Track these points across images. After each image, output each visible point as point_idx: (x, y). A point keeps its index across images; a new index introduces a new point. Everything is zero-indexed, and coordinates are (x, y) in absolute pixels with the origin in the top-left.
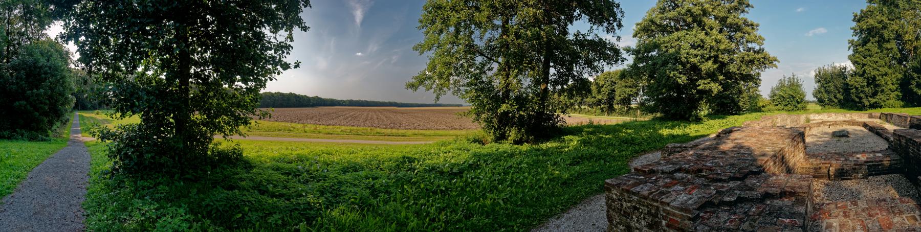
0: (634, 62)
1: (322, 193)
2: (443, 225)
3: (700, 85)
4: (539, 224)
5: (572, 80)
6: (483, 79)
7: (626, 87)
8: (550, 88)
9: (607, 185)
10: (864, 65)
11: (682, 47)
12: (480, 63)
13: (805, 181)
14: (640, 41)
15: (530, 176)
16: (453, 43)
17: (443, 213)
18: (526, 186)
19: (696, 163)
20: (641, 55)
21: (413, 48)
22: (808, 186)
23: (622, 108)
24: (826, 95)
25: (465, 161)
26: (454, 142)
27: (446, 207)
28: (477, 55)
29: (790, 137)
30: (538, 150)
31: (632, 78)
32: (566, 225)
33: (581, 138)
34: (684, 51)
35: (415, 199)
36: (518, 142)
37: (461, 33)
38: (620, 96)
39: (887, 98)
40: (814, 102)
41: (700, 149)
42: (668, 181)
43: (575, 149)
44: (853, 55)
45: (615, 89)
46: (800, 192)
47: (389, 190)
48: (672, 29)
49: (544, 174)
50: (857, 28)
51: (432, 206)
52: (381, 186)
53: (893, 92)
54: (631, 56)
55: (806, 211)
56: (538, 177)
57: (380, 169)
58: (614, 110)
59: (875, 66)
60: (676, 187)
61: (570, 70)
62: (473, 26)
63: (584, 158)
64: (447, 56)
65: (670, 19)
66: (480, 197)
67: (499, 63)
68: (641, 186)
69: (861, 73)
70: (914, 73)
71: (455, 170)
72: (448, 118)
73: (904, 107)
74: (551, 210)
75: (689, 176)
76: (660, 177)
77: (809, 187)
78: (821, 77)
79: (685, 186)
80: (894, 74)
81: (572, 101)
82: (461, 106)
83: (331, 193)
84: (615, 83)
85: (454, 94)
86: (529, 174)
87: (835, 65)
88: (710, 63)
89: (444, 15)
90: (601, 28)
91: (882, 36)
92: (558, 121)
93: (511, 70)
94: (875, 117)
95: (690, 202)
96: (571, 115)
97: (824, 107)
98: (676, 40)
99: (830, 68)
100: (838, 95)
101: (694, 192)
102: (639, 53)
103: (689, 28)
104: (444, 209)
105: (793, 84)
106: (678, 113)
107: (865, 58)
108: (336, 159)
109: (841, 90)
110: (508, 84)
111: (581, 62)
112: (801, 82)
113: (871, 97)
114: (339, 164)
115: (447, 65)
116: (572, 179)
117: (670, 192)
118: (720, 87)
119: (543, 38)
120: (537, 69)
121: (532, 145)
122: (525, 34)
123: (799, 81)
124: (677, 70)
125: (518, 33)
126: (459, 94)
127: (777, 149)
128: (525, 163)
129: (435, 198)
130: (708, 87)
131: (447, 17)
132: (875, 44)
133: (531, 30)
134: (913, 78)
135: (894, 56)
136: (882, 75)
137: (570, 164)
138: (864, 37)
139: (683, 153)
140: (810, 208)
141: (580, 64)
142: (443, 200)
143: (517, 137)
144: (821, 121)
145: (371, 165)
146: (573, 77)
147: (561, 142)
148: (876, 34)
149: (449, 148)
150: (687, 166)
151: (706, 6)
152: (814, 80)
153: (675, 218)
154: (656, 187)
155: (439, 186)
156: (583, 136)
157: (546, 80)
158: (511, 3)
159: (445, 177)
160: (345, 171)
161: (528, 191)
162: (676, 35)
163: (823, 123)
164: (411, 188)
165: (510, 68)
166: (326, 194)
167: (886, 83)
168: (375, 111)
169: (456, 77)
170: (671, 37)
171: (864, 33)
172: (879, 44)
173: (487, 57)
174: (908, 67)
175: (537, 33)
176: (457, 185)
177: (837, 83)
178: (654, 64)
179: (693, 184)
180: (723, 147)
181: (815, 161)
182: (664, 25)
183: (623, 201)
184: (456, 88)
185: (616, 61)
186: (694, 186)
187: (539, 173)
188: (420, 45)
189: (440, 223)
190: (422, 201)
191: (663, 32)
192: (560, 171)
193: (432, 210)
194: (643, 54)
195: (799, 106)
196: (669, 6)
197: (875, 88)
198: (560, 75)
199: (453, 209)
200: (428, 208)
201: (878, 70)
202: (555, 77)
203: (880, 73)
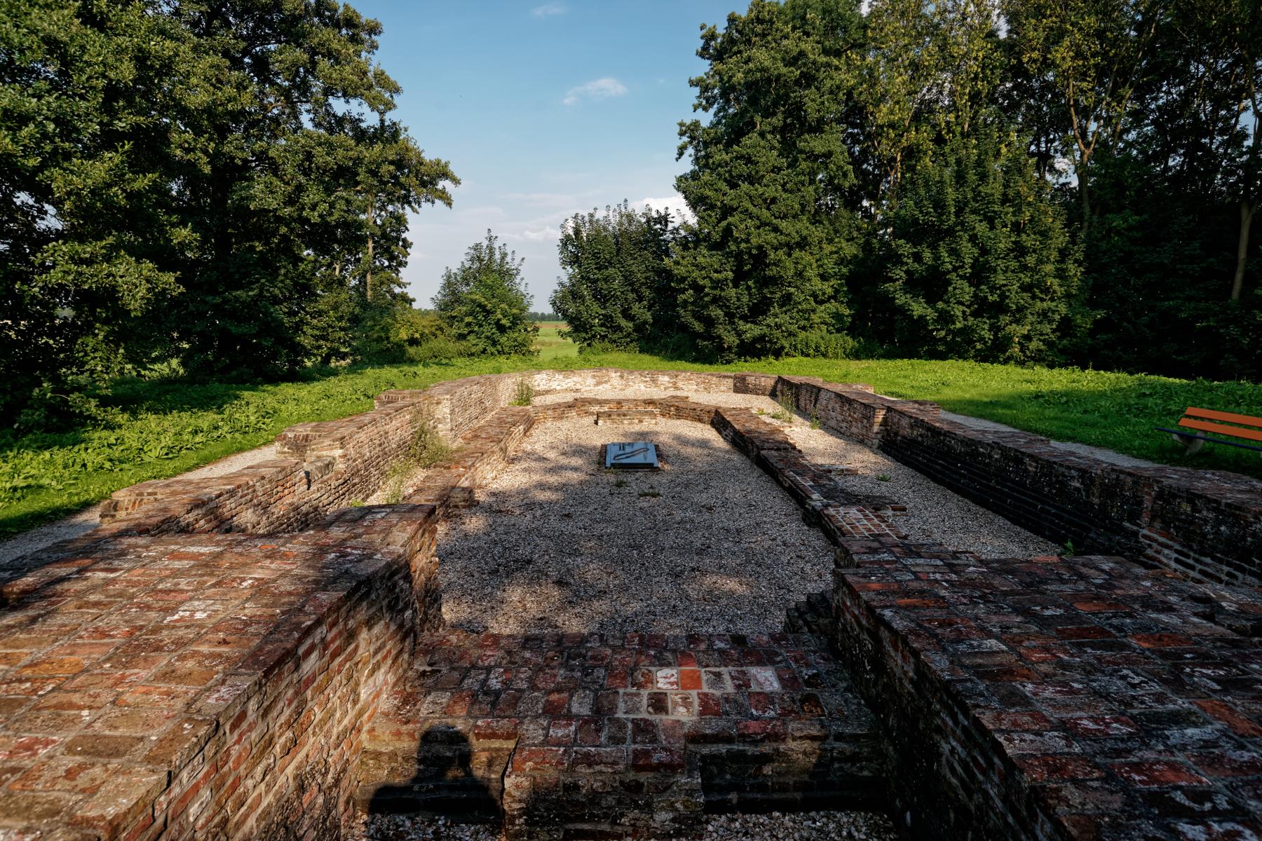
10: (727, 211)
24: (596, 307)
39: (802, 323)
44: (694, 176)
50: (711, 81)
53: (822, 302)
59: (765, 214)
69: (716, 237)
70: (902, 241)
73: (856, 355)
80: (830, 241)
87: (630, 209)
91: (796, 110)
97: (589, 345)
99: (614, 219)
100: (636, 309)
105: (488, 266)
107: (733, 186)
109: (647, 293)
112: (517, 261)
113: (744, 318)
123: (508, 259)
132: (769, 137)
134: (897, 260)
135: (831, 179)
136: (790, 247)
138: (735, 115)
148: (775, 104)
152: (555, 255)
167: (800, 274)
171: (737, 99)
174: (880, 217)
177: (634, 268)
195: (503, 339)
197: (760, 290)
201: (776, 229)
203: (783, 239)
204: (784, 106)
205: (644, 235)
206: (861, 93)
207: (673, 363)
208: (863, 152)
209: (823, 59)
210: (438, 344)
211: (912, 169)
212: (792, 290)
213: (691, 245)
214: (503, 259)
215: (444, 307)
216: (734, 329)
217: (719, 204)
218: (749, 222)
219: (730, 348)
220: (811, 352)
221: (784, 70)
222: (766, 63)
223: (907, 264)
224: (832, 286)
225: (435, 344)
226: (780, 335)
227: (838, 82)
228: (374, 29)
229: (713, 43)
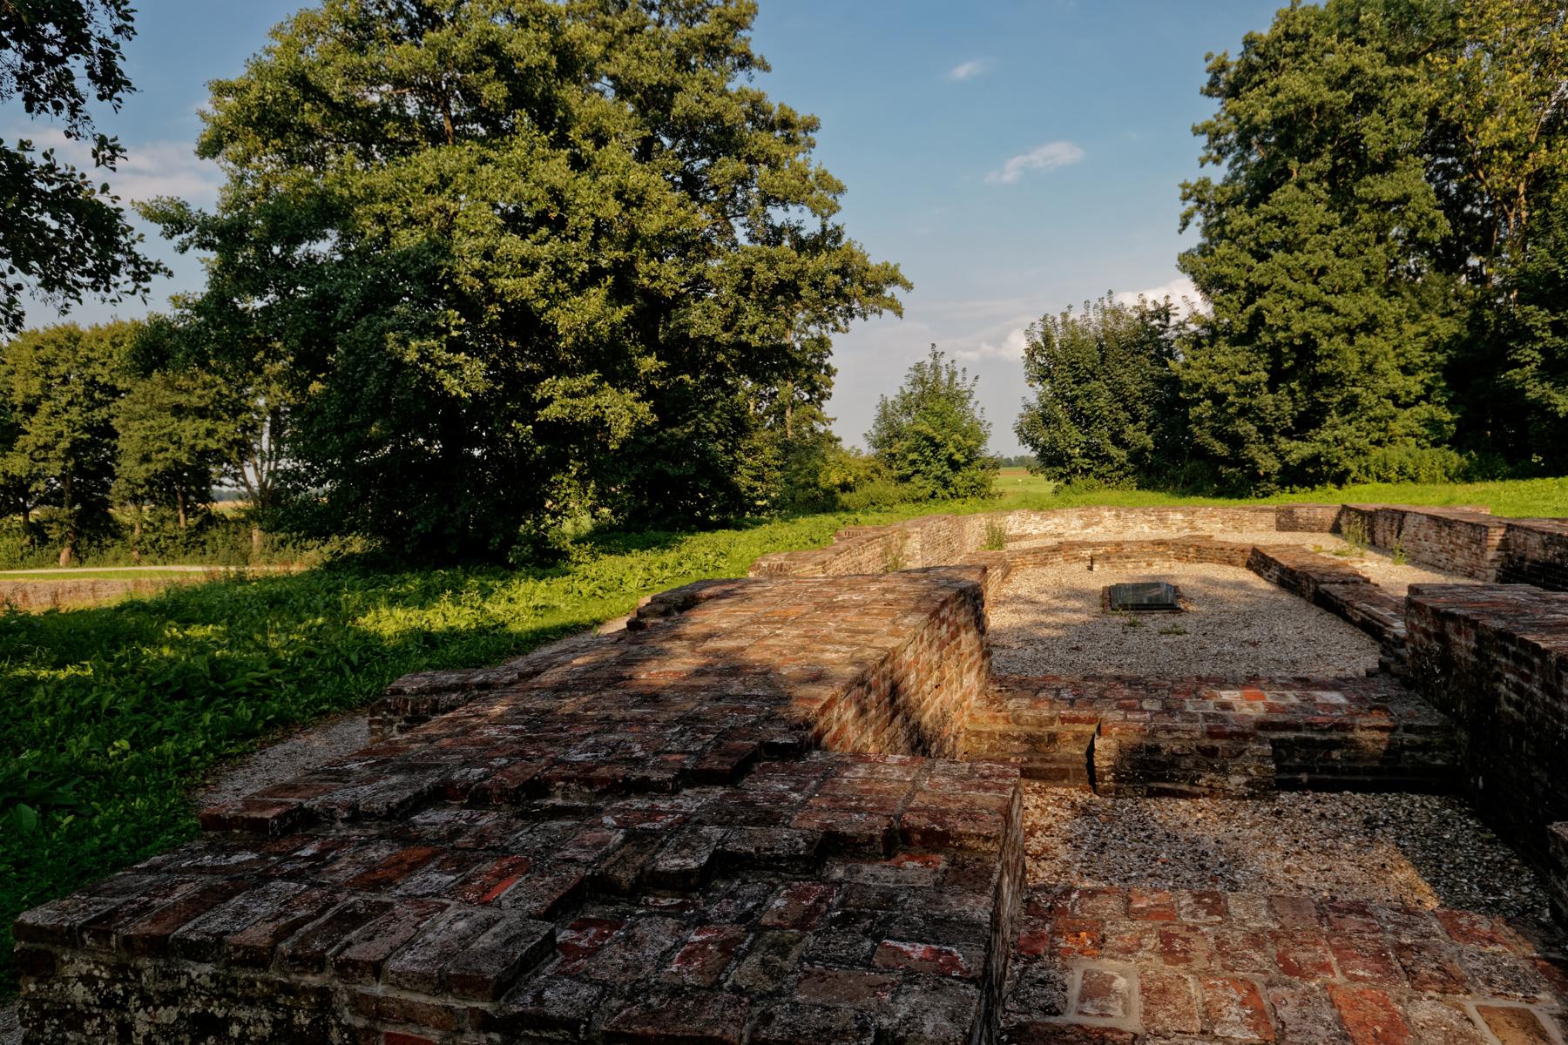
0: (213, 284)
3: (551, 400)
7: (178, 411)
9: (28, 939)
10: (1256, 291)
11: (460, 220)
13: (987, 789)
14: (242, 178)
19: (522, 754)
20: (251, 252)
22: (999, 810)
23: (163, 520)
24: (1075, 434)
29: (923, 606)
31: (203, 364)
34: (467, 244)
38: (146, 459)
39: (1376, 436)
40: (1021, 461)
41: (542, 689)
42: (380, 853)
44: (1204, 251)
45: (114, 422)
46: (970, 836)
48: (409, 131)
50: (1223, 125)
53: (1406, 406)
54: (194, 253)
55: (995, 916)
58: (115, 531)
59: (1311, 290)
60: (417, 879)
65: (399, 82)
68: (238, 901)
69: (1241, 327)
70: (1528, 309)
73: (1466, 476)
75: (487, 820)
76: (344, 842)
77: (1006, 814)
78: (1052, 357)
79: (461, 864)
80: (1415, 319)
84: (114, 392)
87: (1117, 301)
88: (595, 299)
91: (1352, 146)
94: (1310, 527)
95: (486, 940)
97: (1068, 482)
98: (429, 189)
99: (1095, 317)
100: (1130, 432)
101: (506, 891)
102: (242, 241)
103: (496, 131)
105: (933, 391)
106: (450, 530)
107: (1262, 257)
109: (1145, 410)
112: (969, 382)
113: (1287, 433)
117: (389, 906)
118: (643, 408)
123: (958, 379)
124: (439, 332)
127: (868, 652)
130: (586, 409)
132: (1311, 186)
135: (1413, 232)
136: (1350, 333)
138: (1260, 164)
139: (462, 712)
140: (1011, 906)
144: (1051, 542)
148: (1319, 142)
150: (477, 772)
151: (575, 30)
153: (413, 1031)
154: (316, 894)
162: (428, 161)
163: (1064, 549)
167: (1369, 369)
170: (407, 173)
171: (1261, 143)
172: (1333, 184)
174: (1497, 280)
177: (1125, 378)
178: (324, 302)
179: (505, 852)
180: (651, 674)
181: (1030, 707)
182: (370, 108)
183: (134, 1001)
186: (506, 863)
191: (367, 144)
194: (262, 246)
195: (957, 479)
196: (392, 16)
197: (1308, 393)
201: (1328, 309)
203: (1339, 321)
204: (1331, 142)
205: (1137, 335)
206: (1451, 108)
207: (1186, 500)
208: (1463, 188)
209: (1390, 71)
210: (878, 487)
211: (1544, 203)
212: (1358, 390)
213: (1205, 341)
214: (951, 379)
215: (880, 443)
216: (1273, 450)
217: (1242, 283)
218: (1288, 303)
219: (1267, 475)
220: (1393, 475)
221: (1329, 96)
222: (1302, 91)
223: (1543, 340)
224: (1422, 382)
225: (870, 489)
226: (1342, 454)
227: (1413, 100)
228: (811, 126)
229: (1223, 76)
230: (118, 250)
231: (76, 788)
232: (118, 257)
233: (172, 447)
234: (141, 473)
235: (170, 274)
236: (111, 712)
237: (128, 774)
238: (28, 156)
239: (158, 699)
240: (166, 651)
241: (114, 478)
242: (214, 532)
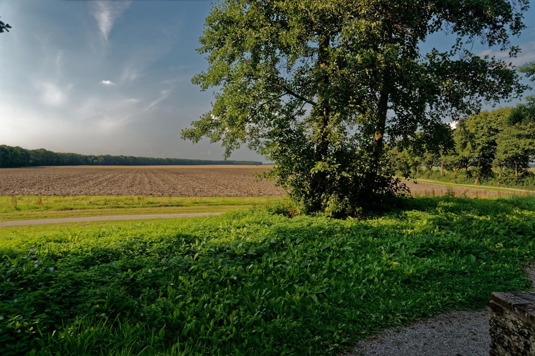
1: (40, 307)
2: (234, 329)
4: (370, 335)
5: (421, 127)
6: (291, 127)
7: (519, 136)
8: (386, 137)
12: (287, 105)
15: (357, 265)
16: (249, 75)
17: (234, 312)
18: (351, 278)
21: (192, 80)
23: (509, 173)
25: (265, 240)
26: (251, 213)
27: (238, 304)
28: (283, 93)
30: (366, 228)
32: (412, 344)
33: (434, 217)
35: (194, 294)
36: (340, 215)
37: (261, 61)
38: (506, 152)
43: (425, 232)
45: (496, 141)
47: (157, 282)
49: (376, 263)
51: (219, 303)
52: (146, 278)
56: (367, 267)
57: (147, 254)
58: (493, 176)
61: (419, 110)
62: (278, 51)
63: (440, 248)
64: (240, 93)
66: (285, 289)
67: (314, 104)
71: (252, 252)
72: (242, 180)
74: (387, 318)
81: (417, 159)
82: (261, 164)
83: (60, 303)
84: (497, 131)
85: (251, 148)
86: (355, 261)
89: (236, 33)
90: (477, 39)
92: (397, 188)
93: (330, 113)
96: (418, 180)
104: (235, 307)
108: (72, 248)
110: (326, 134)
111: (439, 98)
114: (77, 255)
115: (242, 106)
116: (420, 278)
119: (381, 64)
120: (369, 110)
121: (359, 220)
122: (352, 60)
125: (343, 58)
126: (258, 147)
128: (349, 245)
129: (223, 292)
131: (241, 37)
133: (362, 53)
137: (416, 255)
141: (437, 101)
142: (235, 294)
143: (337, 208)
145: (133, 250)
146: (424, 122)
147: (401, 219)
149: (243, 221)
155: (228, 275)
156: (437, 213)
157: (382, 129)
158: (333, 14)
159: (238, 262)
160: (87, 263)
161: (354, 286)
164: (189, 279)
165: (328, 110)
166: (50, 307)
168: (142, 171)
169: (253, 125)
173: (297, 96)
175: (371, 57)
176: (253, 272)
184: (254, 140)
185: (506, 93)
187: (368, 260)
188: (202, 76)
189: (230, 327)
190: (205, 297)
192: (400, 262)
193: (219, 309)
198: (403, 120)
199: (248, 306)
200: (213, 306)
202: (394, 123)
230: (512, 84)
231: (486, 254)
232: (512, 86)
233: (516, 149)
234: (503, 157)
235: (531, 89)
236: (497, 234)
237: (502, 255)
238: (487, 60)
239: (513, 234)
240: (514, 217)
241: (494, 158)
242: (528, 178)
